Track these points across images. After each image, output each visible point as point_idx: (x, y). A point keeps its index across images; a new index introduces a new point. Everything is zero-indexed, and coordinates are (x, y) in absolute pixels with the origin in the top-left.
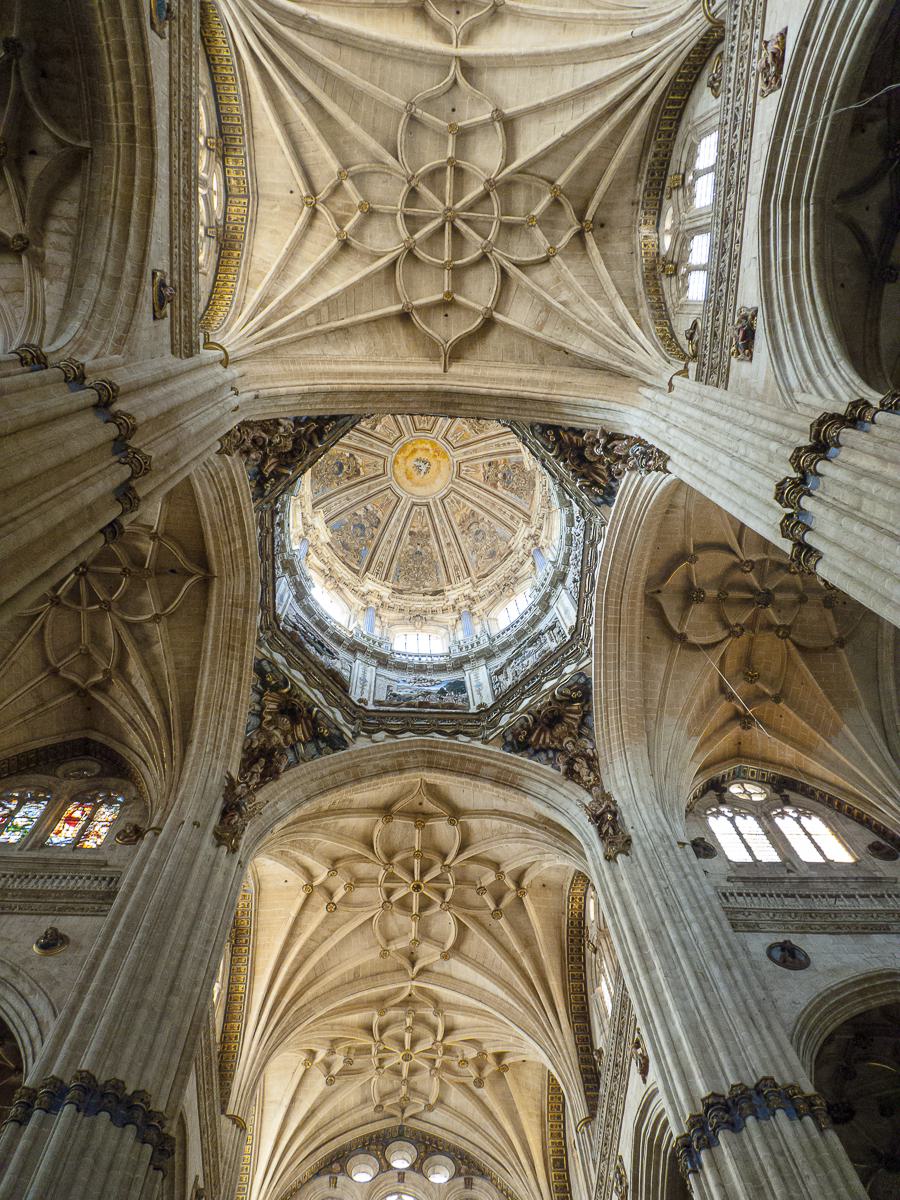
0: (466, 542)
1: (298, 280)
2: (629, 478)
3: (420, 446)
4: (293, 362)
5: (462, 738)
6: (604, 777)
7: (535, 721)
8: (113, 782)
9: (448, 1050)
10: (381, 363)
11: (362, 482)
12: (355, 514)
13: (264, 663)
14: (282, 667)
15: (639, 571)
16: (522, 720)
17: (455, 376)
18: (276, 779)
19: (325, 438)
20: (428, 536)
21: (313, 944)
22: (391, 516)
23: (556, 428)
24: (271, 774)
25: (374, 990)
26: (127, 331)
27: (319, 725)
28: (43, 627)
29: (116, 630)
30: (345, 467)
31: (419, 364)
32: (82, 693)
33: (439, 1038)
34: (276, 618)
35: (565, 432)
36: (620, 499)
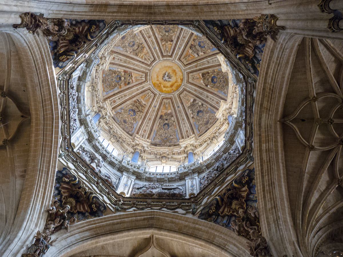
2: (49, 202)
3: (169, 89)
11: (200, 70)
12: (204, 53)
13: (253, 71)
15: (37, 135)
16: (95, 36)
17: (148, 233)
18: (247, 20)
19: (215, 202)
20: (162, 40)
23: (93, 214)
24: (250, 24)
27: (220, 34)
30: (210, 80)
35: (87, 211)
36: (53, 180)
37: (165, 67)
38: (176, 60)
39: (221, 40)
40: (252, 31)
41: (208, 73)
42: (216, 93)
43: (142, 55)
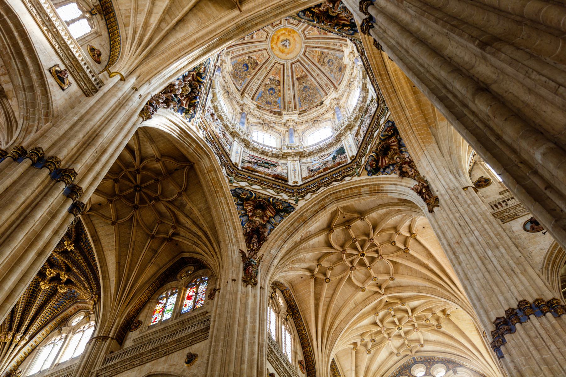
0: (325, 69)
1: (146, 10)
3: (279, 34)
4: (163, 53)
5: (347, 179)
6: (419, 170)
7: (377, 155)
8: (201, 272)
9: (418, 318)
10: (207, 26)
11: (261, 67)
12: (266, 84)
13: (237, 190)
14: (247, 188)
16: (371, 158)
18: (266, 241)
20: (306, 76)
21: (328, 300)
22: (284, 76)
24: (262, 240)
25: (367, 307)
26: (48, 108)
28: (137, 220)
29: (167, 207)
30: (249, 65)
31: (226, 15)
32: (170, 240)
33: (410, 314)
34: (235, 166)
35: (314, 8)
37: (292, 52)
38: (285, 63)
39: (273, 200)
40: (257, 236)
41: (254, 69)
42: (239, 58)
43: (317, 54)
